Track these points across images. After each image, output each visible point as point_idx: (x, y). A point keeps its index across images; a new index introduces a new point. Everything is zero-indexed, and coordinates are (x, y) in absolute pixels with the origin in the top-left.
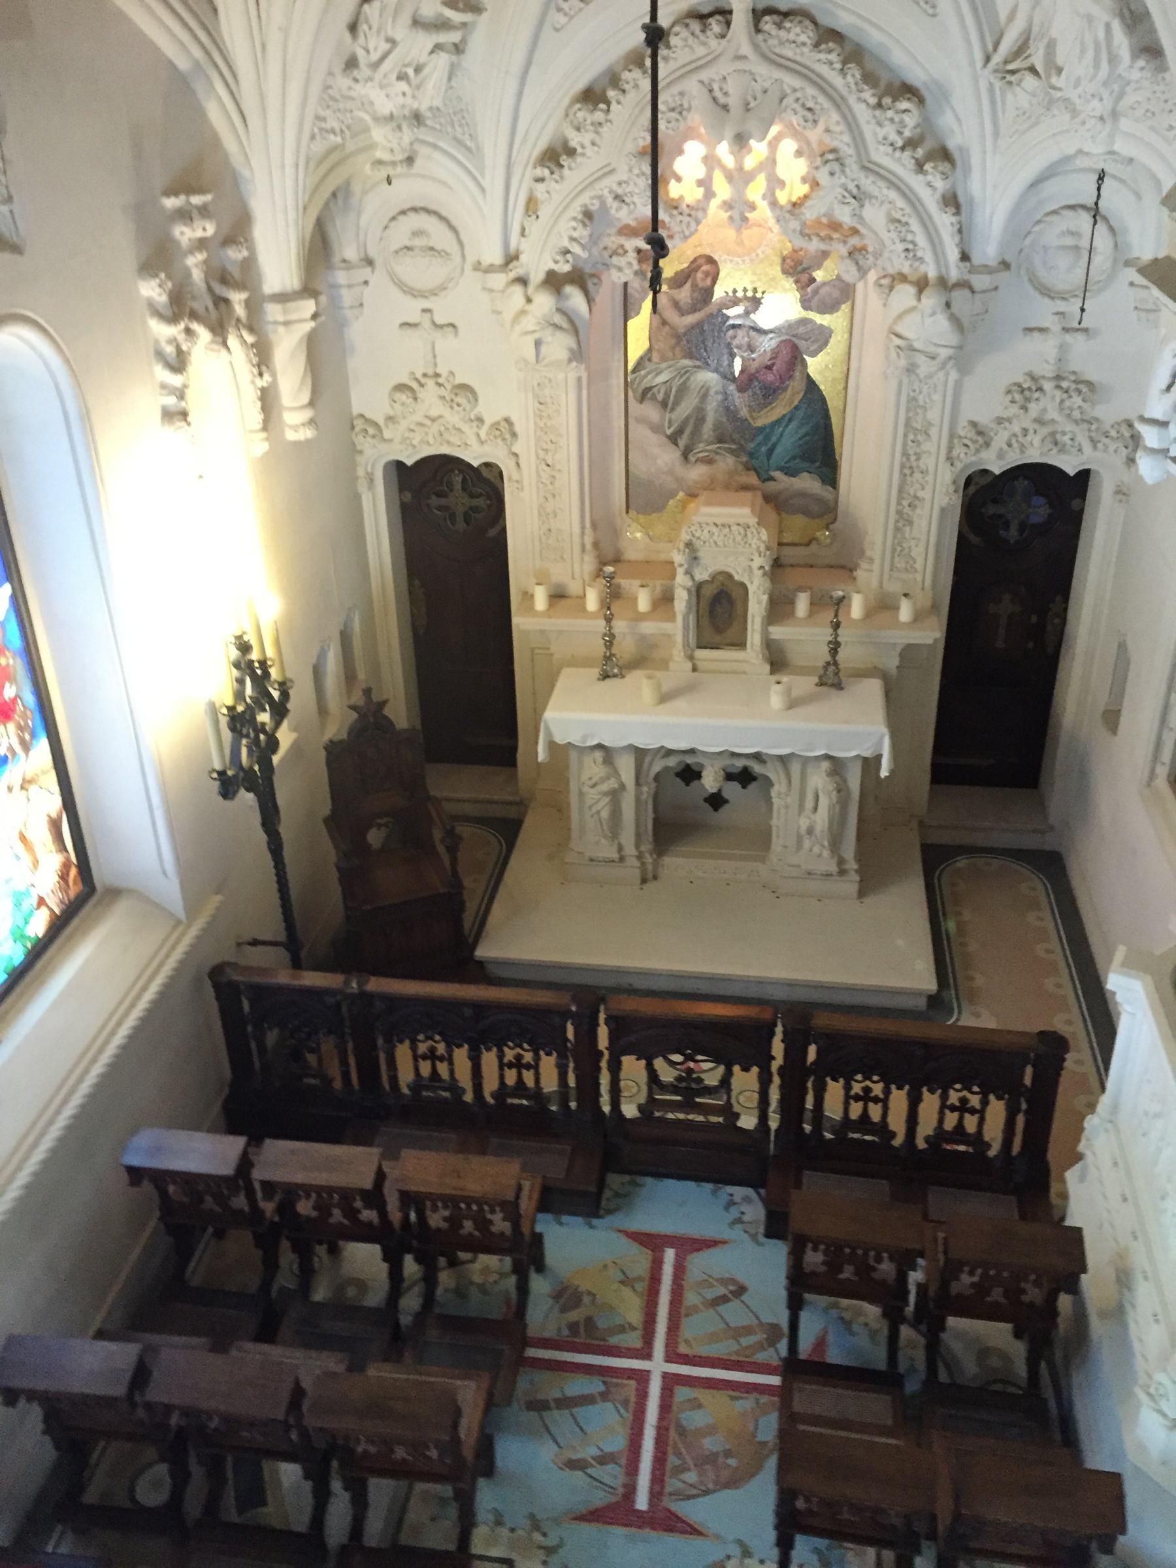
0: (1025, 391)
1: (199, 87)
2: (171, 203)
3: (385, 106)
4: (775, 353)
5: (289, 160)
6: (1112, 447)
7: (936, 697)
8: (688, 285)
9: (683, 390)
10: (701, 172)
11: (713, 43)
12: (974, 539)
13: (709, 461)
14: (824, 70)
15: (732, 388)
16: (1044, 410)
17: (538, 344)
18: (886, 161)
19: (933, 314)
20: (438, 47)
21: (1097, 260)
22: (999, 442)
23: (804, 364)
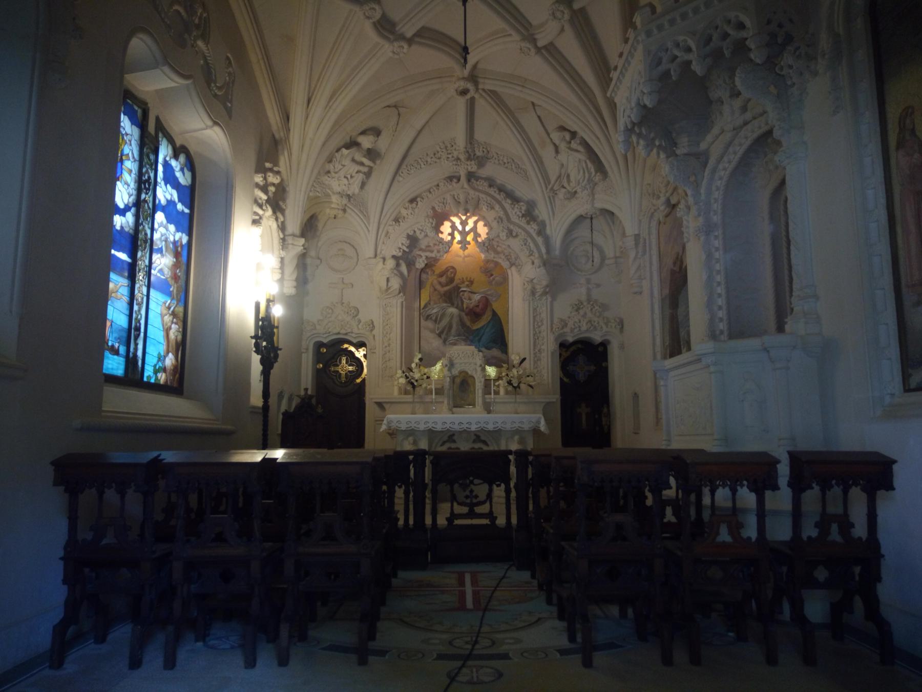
0: (578, 307)
1: (280, 147)
2: (268, 165)
3: (337, 189)
4: (479, 302)
5: (303, 189)
6: (613, 325)
7: (560, 433)
8: (444, 277)
9: (443, 315)
10: (450, 230)
11: (454, 184)
12: (565, 379)
13: (455, 344)
14: (492, 193)
15: (463, 314)
16: (585, 314)
17: (388, 280)
18: (517, 221)
19: (539, 267)
20: (358, 172)
21: (595, 260)
22: (570, 324)
23: (491, 305)
